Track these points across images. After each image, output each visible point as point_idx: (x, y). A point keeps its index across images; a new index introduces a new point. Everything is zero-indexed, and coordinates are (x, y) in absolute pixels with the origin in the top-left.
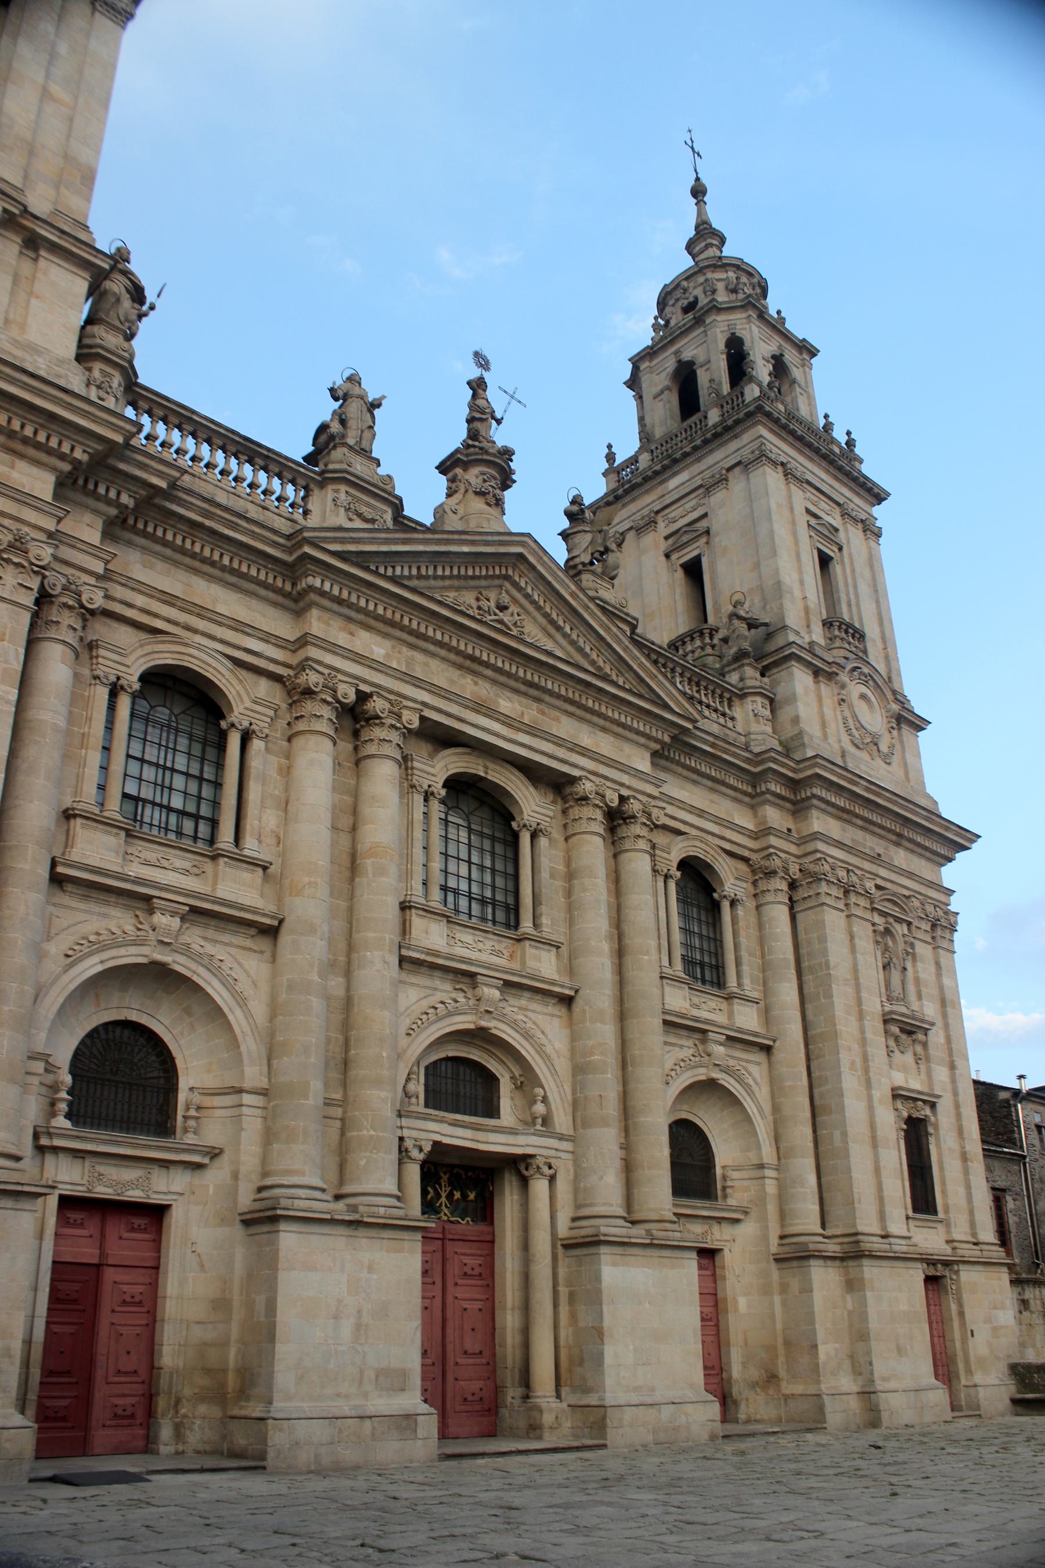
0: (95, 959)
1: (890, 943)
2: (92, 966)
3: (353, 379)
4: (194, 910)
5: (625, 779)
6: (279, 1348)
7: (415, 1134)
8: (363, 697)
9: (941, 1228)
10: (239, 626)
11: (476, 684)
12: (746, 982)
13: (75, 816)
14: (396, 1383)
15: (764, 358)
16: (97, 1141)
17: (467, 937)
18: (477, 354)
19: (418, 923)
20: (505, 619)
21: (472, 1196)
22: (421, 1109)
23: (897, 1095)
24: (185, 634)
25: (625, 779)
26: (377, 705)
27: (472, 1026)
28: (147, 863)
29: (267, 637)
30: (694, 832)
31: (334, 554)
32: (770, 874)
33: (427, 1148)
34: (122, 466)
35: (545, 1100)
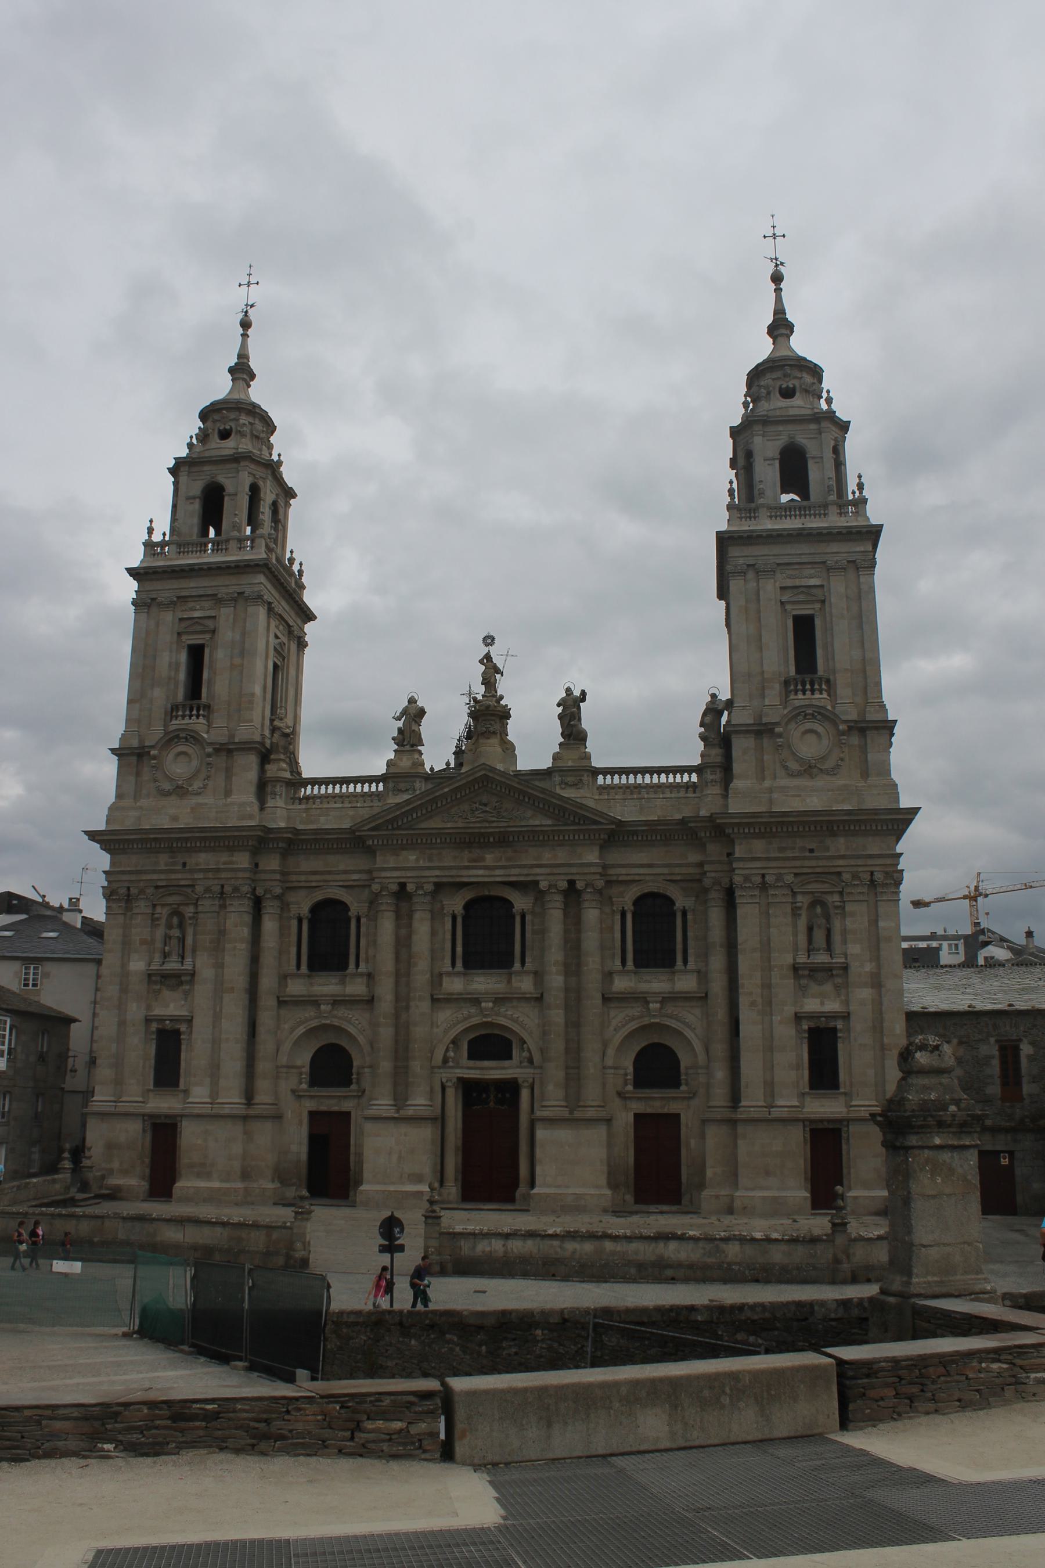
0: (301, 1027)
1: (819, 910)
2: (301, 1030)
3: (412, 701)
4: (335, 1001)
5: (574, 870)
6: (365, 1166)
7: (448, 1075)
8: (402, 886)
9: (842, 1099)
10: (345, 872)
11: (470, 852)
12: (691, 960)
13: (287, 976)
14: (418, 1178)
15: (765, 460)
16: (316, 1091)
17: (481, 979)
18: (485, 639)
19: (445, 979)
20: (487, 809)
21: (508, 1095)
22: (464, 1061)
23: (798, 1018)
24: (325, 884)
25: (574, 870)
26: (410, 888)
27: (481, 1021)
29: (360, 872)
30: (648, 878)
31: (369, 830)
32: (706, 891)
33: (455, 1080)
34: (271, 836)
35: (529, 1051)
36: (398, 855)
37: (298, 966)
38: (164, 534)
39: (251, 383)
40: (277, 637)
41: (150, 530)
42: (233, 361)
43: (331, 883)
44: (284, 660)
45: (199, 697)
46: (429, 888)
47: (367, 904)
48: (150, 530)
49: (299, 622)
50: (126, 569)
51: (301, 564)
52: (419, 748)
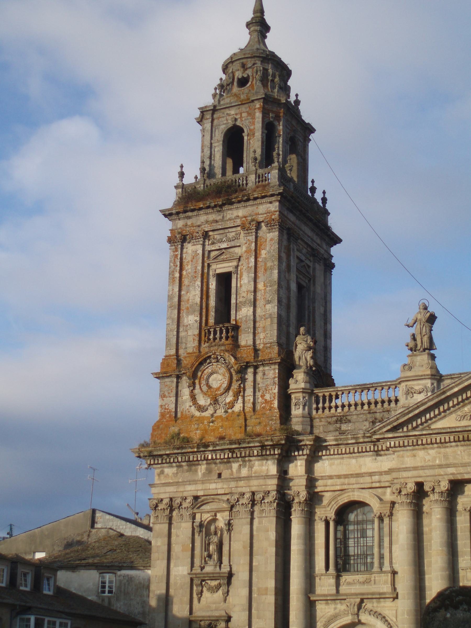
8: (420, 485)
28: (349, 584)
36: (415, 456)
37: (327, 568)
38: (196, 177)
39: (267, 34)
40: (298, 258)
41: (182, 175)
42: (249, 16)
43: (355, 486)
44: (309, 281)
45: (229, 320)
46: (444, 485)
47: (389, 505)
48: (182, 175)
49: (325, 246)
50: (161, 211)
51: (324, 192)
52: (432, 352)
